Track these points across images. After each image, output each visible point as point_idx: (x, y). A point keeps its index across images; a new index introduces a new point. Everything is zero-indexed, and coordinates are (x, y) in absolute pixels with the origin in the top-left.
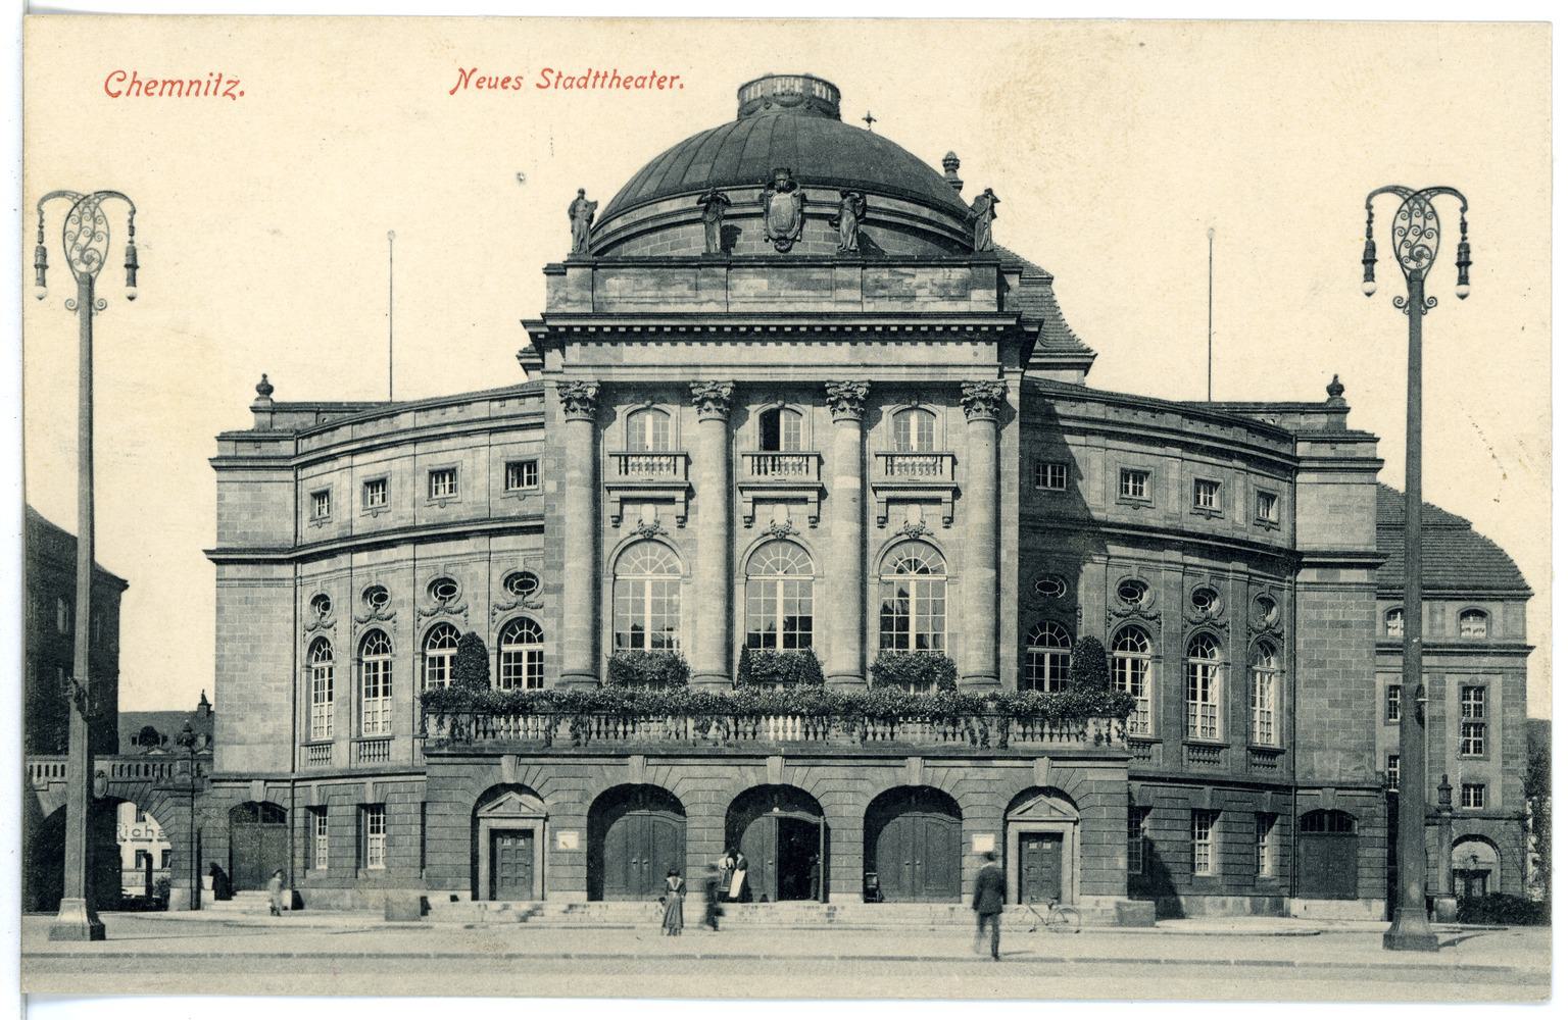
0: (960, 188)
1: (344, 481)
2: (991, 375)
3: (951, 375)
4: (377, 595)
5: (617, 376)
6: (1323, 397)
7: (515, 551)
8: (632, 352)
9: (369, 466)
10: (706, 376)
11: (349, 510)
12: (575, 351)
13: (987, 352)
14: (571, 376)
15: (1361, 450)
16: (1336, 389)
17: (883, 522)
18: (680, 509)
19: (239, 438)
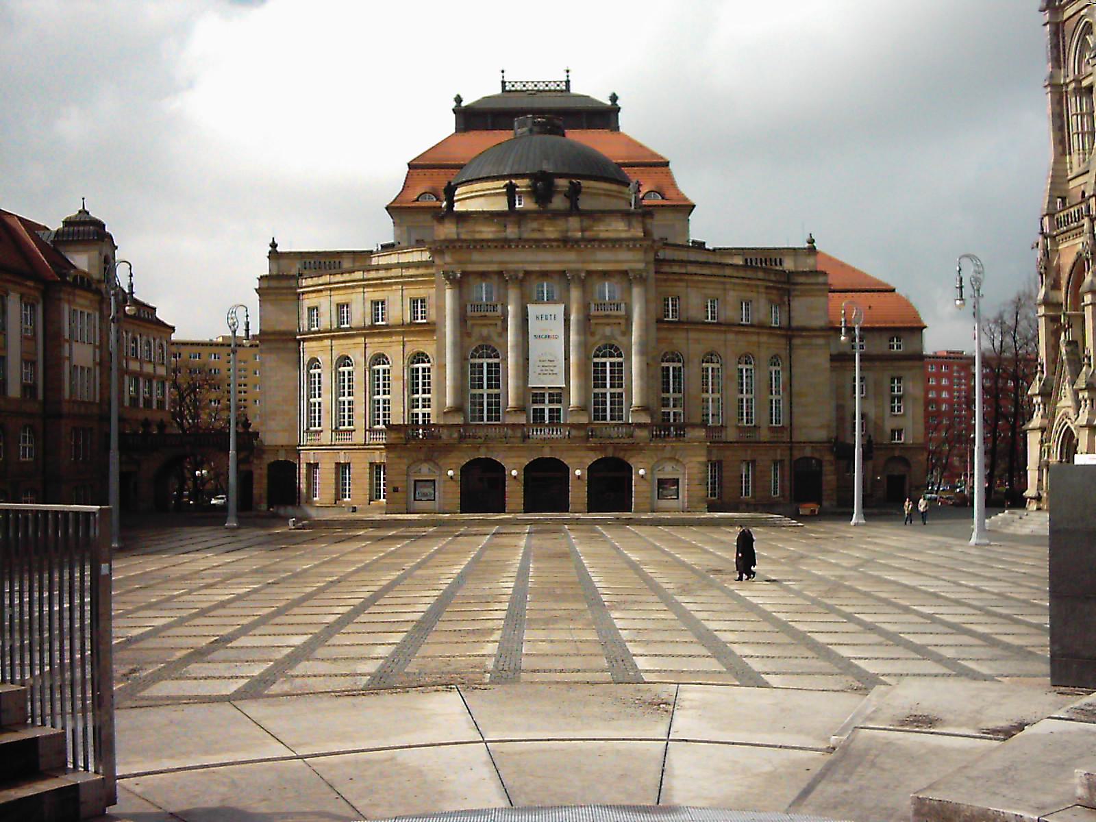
0: (619, 111)
1: (326, 304)
2: (641, 266)
3: (625, 267)
4: (345, 360)
5: (470, 268)
6: (807, 245)
8: (476, 256)
9: (339, 297)
10: (512, 267)
11: (326, 320)
12: (448, 258)
13: (639, 255)
14: (447, 268)
15: (821, 279)
16: (811, 241)
17: (593, 334)
18: (499, 329)
19: (262, 278)
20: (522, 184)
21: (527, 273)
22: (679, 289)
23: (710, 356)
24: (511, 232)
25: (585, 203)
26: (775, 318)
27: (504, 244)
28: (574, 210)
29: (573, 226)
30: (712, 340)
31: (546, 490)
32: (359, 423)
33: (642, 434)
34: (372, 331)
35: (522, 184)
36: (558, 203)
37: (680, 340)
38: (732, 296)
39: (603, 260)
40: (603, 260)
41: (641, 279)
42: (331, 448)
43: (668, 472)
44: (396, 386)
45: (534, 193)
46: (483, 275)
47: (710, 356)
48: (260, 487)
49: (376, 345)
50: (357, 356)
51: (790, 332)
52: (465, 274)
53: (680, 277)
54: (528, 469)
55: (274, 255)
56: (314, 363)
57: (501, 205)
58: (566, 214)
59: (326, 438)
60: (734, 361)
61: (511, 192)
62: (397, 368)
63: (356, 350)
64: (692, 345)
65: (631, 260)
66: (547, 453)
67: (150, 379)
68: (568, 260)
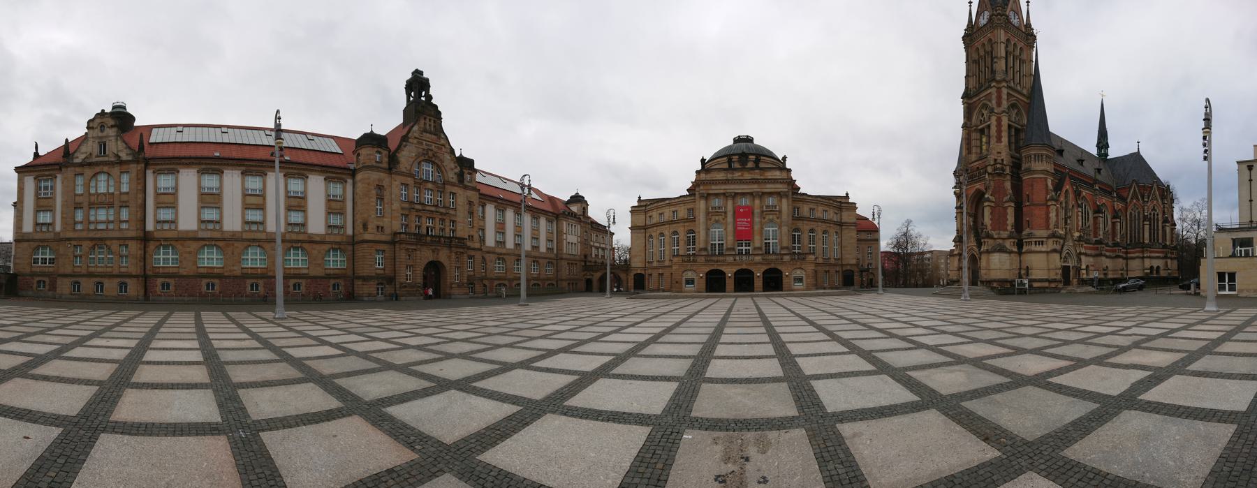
1: (655, 214)
4: (662, 234)
7: (689, 226)
20: (735, 158)
21: (736, 194)
22: (800, 205)
23: (812, 231)
24: (730, 176)
25: (761, 165)
26: (836, 218)
27: (726, 182)
28: (757, 167)
29: (756, 175)
30: (813, 225)
31: (744, 283)
32: (667, 258)
33: (787, 258)
34: (672, 222)
35: (735, 158)
36: (750, 165)
37: (800, 224)
38: (820, 208)
39: (770, 188)
40: (770, 188)
41: (787, 196)
42: (656, 268)
43: (798, 273)
44: (681, 243)
45: (739, 161)
46: (717, 195)
47: (812, 231)
48: (631, 283)
49: (674, 227)
50: (666, 233)
51: (841, 224)
52: (709, 195)
53: (800, 201)
54: (735, 273)
55: (640, 200)
56: (651, 236)
57: (726, 166)
58: (752, 169)
59: (655, 264)
60: (820, 233)
61: (730, 162)
62: (682, 236)
63: (667, 231)
64: (805, 227)
65: (781, 188)
66: (744, 267)
67: (597, 248)
68: (754, 188)
